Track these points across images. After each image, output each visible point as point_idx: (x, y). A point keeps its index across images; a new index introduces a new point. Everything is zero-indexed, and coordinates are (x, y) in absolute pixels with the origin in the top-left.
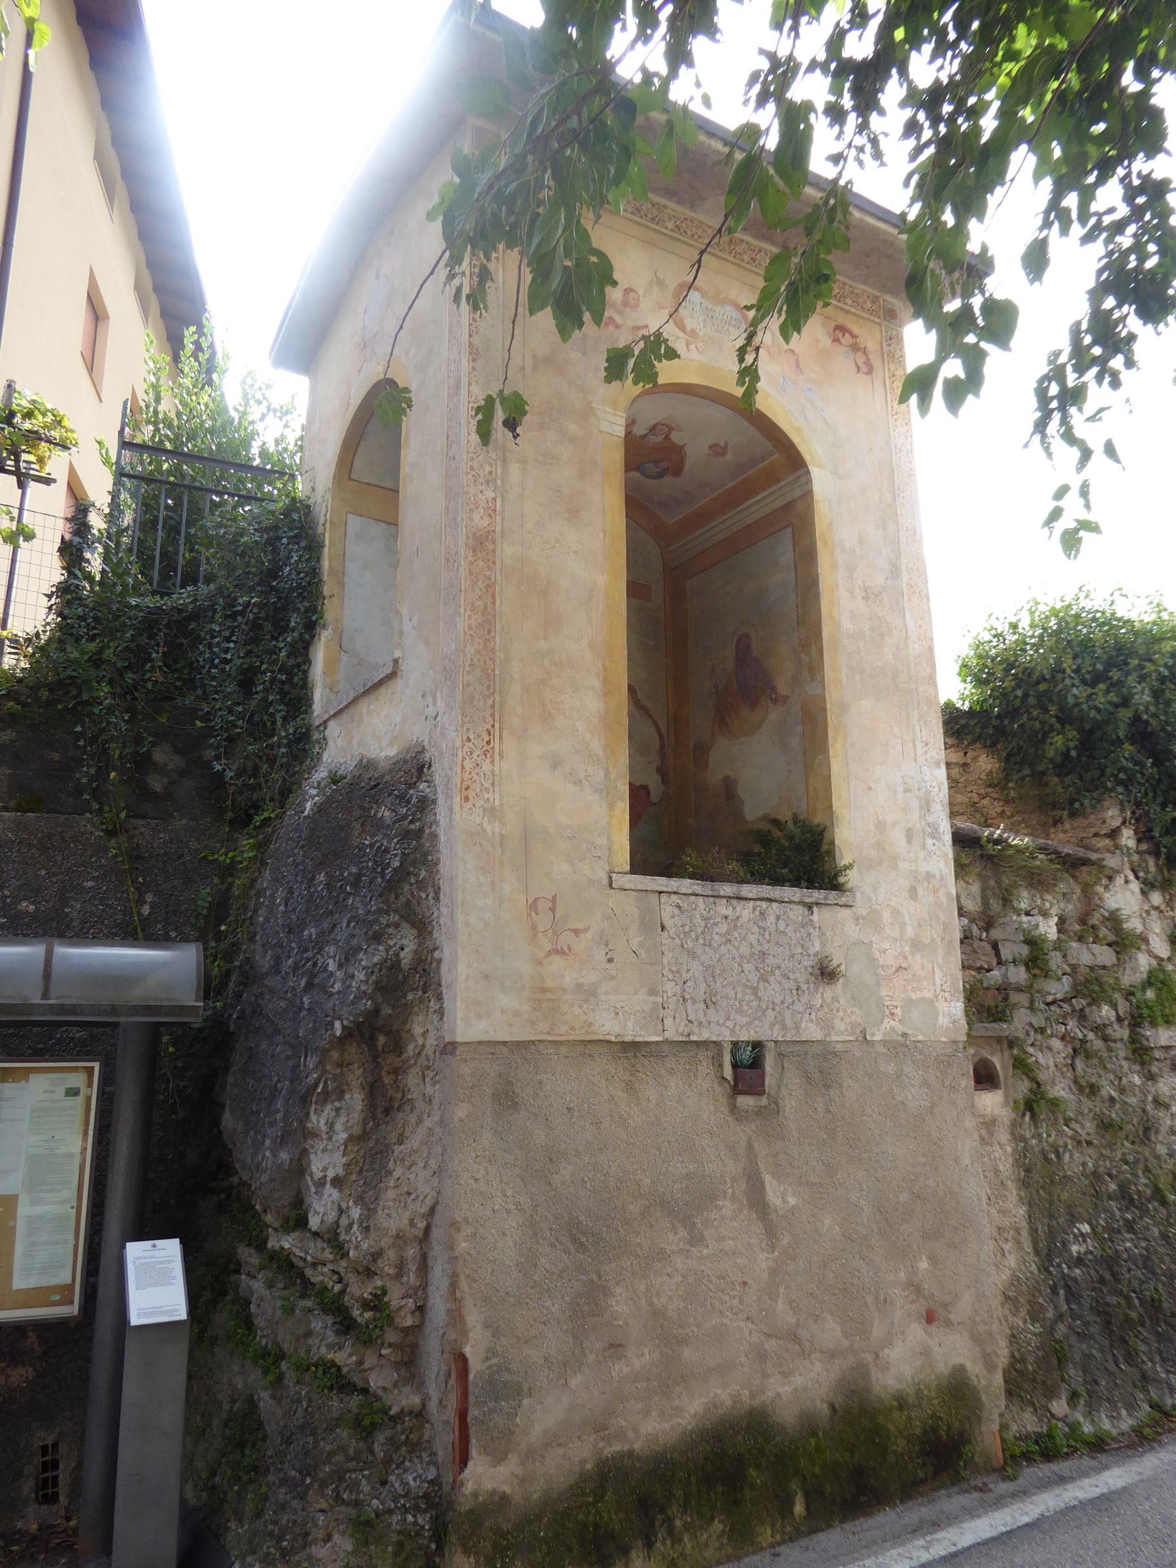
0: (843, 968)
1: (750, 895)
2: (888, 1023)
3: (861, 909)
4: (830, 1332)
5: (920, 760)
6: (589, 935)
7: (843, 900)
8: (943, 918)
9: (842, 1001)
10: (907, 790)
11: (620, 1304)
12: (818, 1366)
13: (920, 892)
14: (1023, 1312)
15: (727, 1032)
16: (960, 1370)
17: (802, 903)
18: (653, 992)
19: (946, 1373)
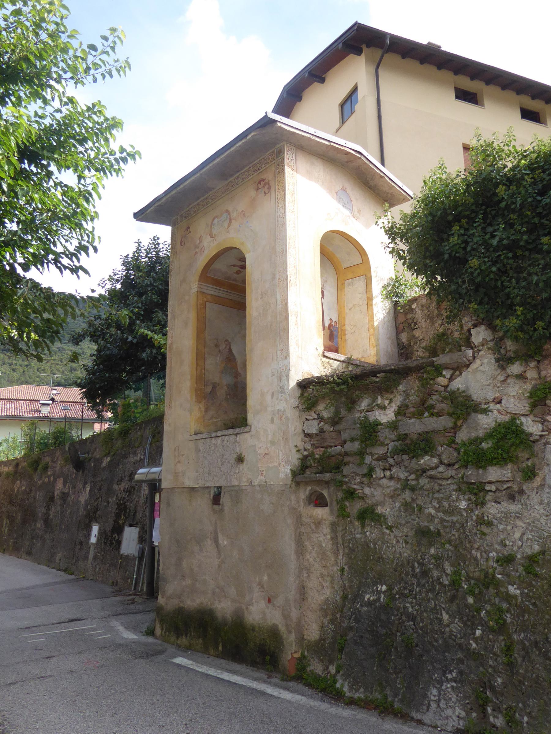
0: (246, 457)
1: (219, 435)
2: (260, 478)
3: (253, 432)
4: (232, 591)
5: (279, 359)
6: (184, 456)
7: (246, 430)
8: (283, 429)
9: (245, 470)
10: (273, 375)
11: (185, 564)
12: (229, 603)
13: (275, 419)
14: (329, 618)
15: (213, 483)
16: (275, 626)
17: (233, 434)
18: (197, 472)
19: (270, 625)
